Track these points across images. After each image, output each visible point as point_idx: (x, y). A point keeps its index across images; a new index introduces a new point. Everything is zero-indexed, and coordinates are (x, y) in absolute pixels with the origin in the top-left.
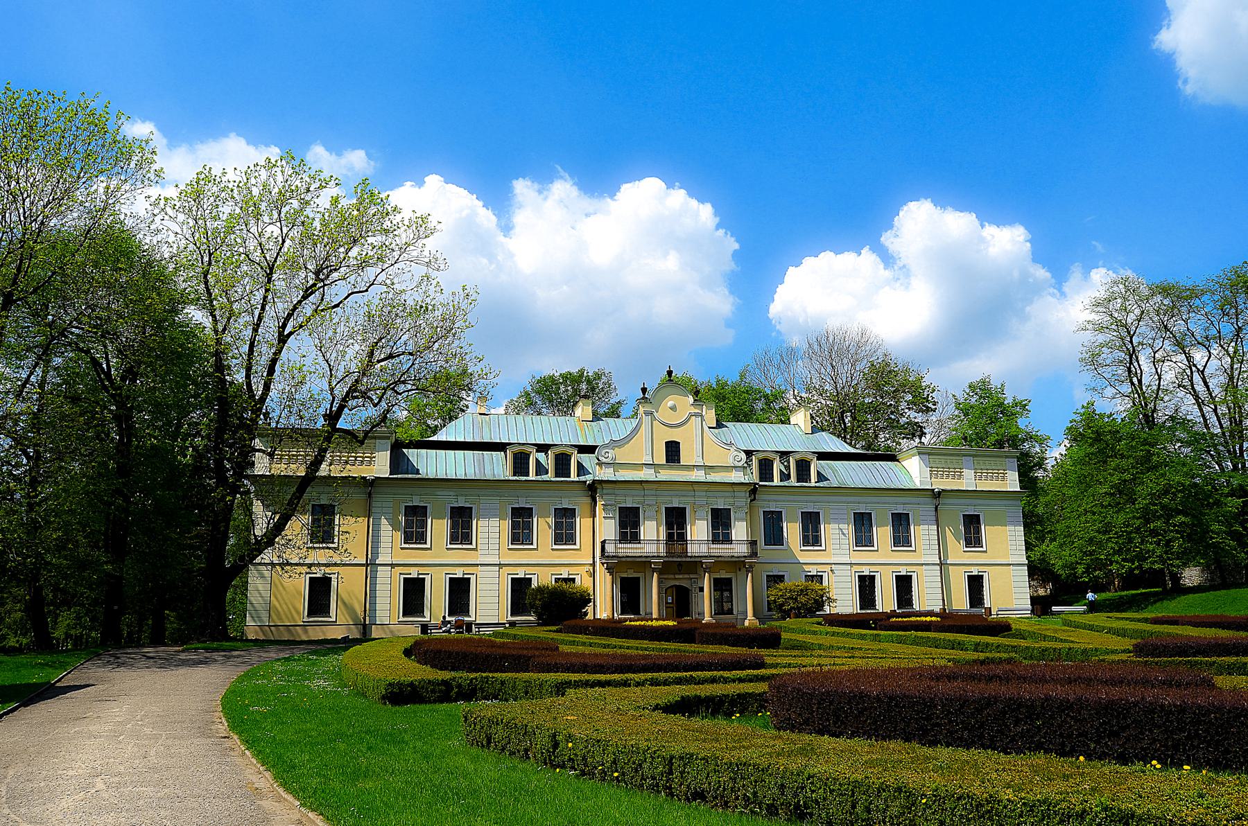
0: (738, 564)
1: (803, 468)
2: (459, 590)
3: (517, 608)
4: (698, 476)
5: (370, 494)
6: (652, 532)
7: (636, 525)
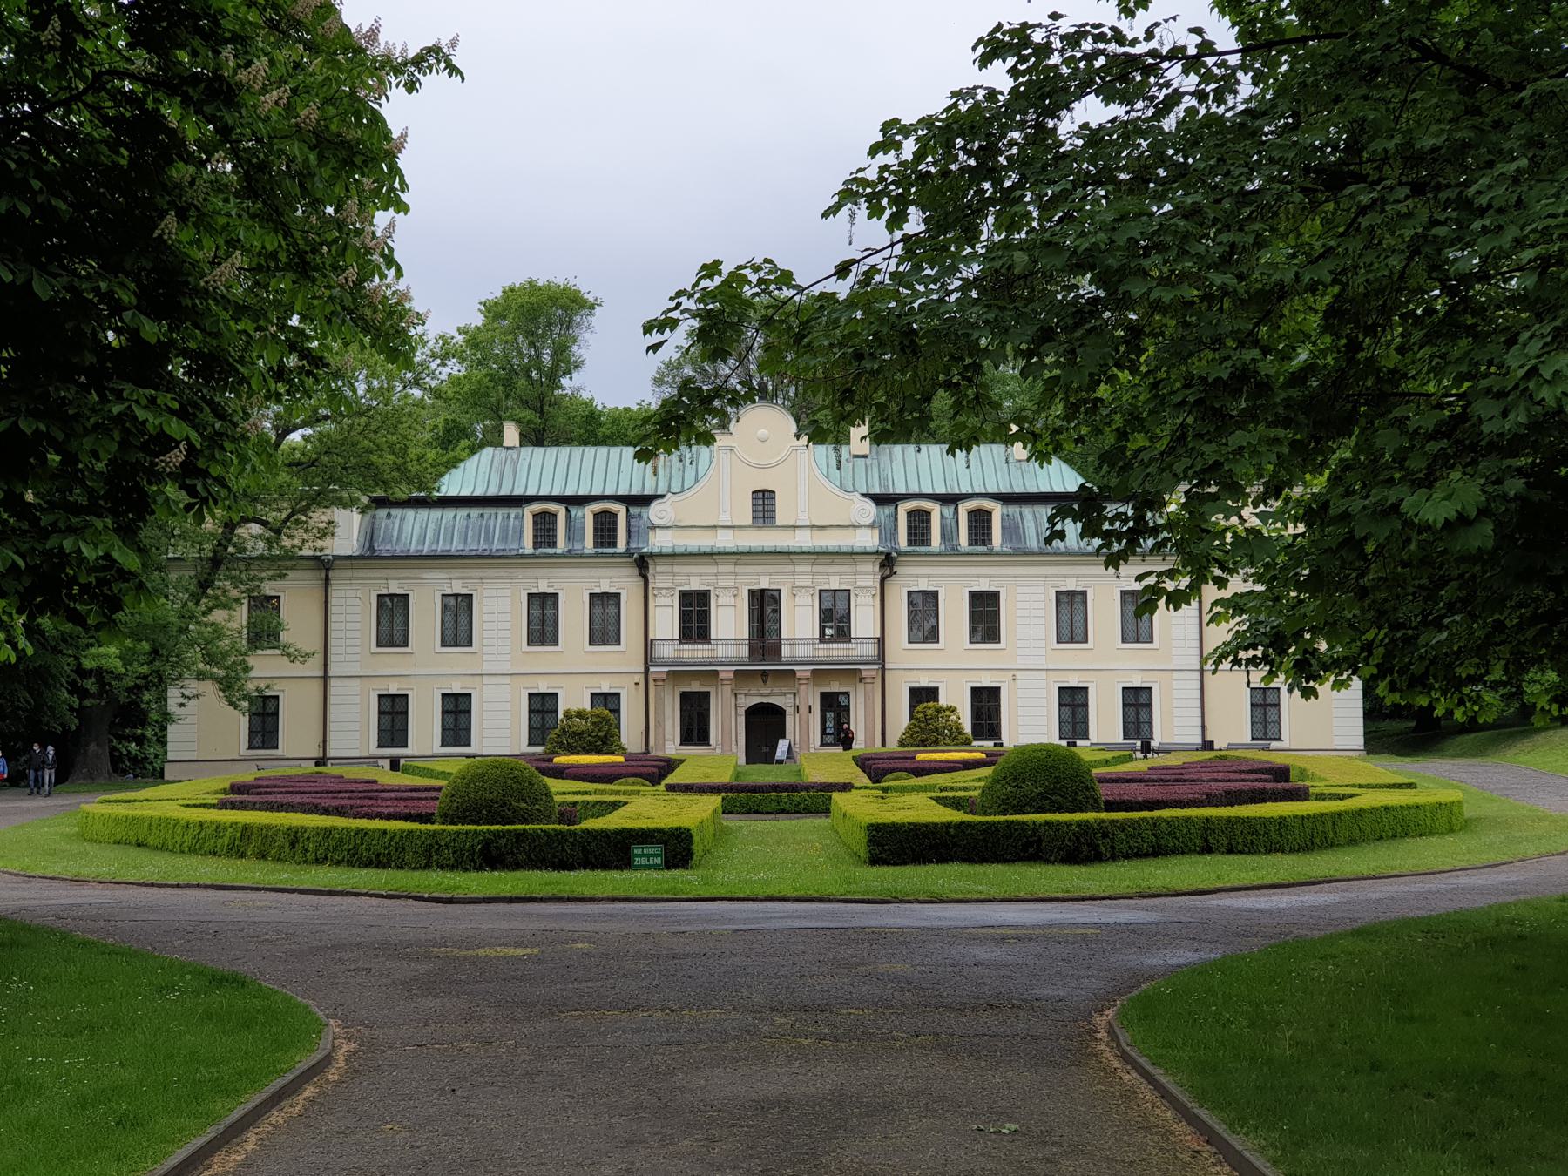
0: (852, 674)
1: (980, 521)
2: (457, 710)
3: (537, 734)
4: (803, 540)
5: (327, 579)
6: (730, 622)
7: (704, 616)
